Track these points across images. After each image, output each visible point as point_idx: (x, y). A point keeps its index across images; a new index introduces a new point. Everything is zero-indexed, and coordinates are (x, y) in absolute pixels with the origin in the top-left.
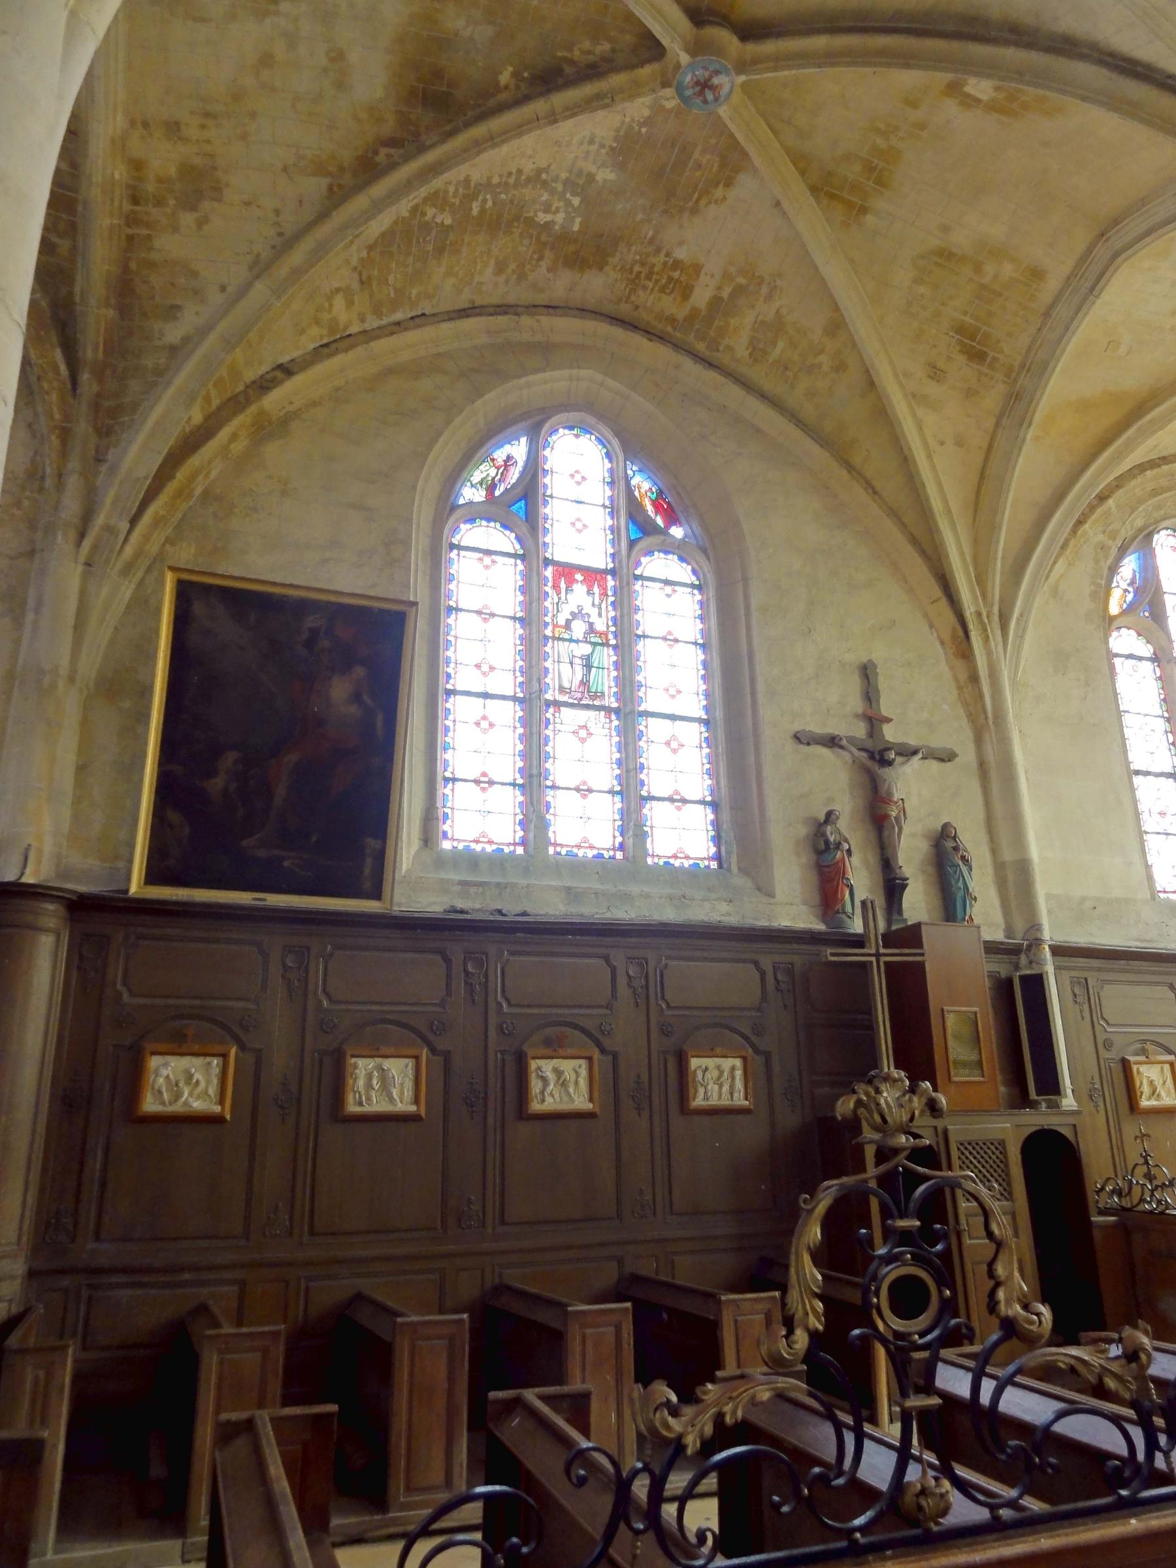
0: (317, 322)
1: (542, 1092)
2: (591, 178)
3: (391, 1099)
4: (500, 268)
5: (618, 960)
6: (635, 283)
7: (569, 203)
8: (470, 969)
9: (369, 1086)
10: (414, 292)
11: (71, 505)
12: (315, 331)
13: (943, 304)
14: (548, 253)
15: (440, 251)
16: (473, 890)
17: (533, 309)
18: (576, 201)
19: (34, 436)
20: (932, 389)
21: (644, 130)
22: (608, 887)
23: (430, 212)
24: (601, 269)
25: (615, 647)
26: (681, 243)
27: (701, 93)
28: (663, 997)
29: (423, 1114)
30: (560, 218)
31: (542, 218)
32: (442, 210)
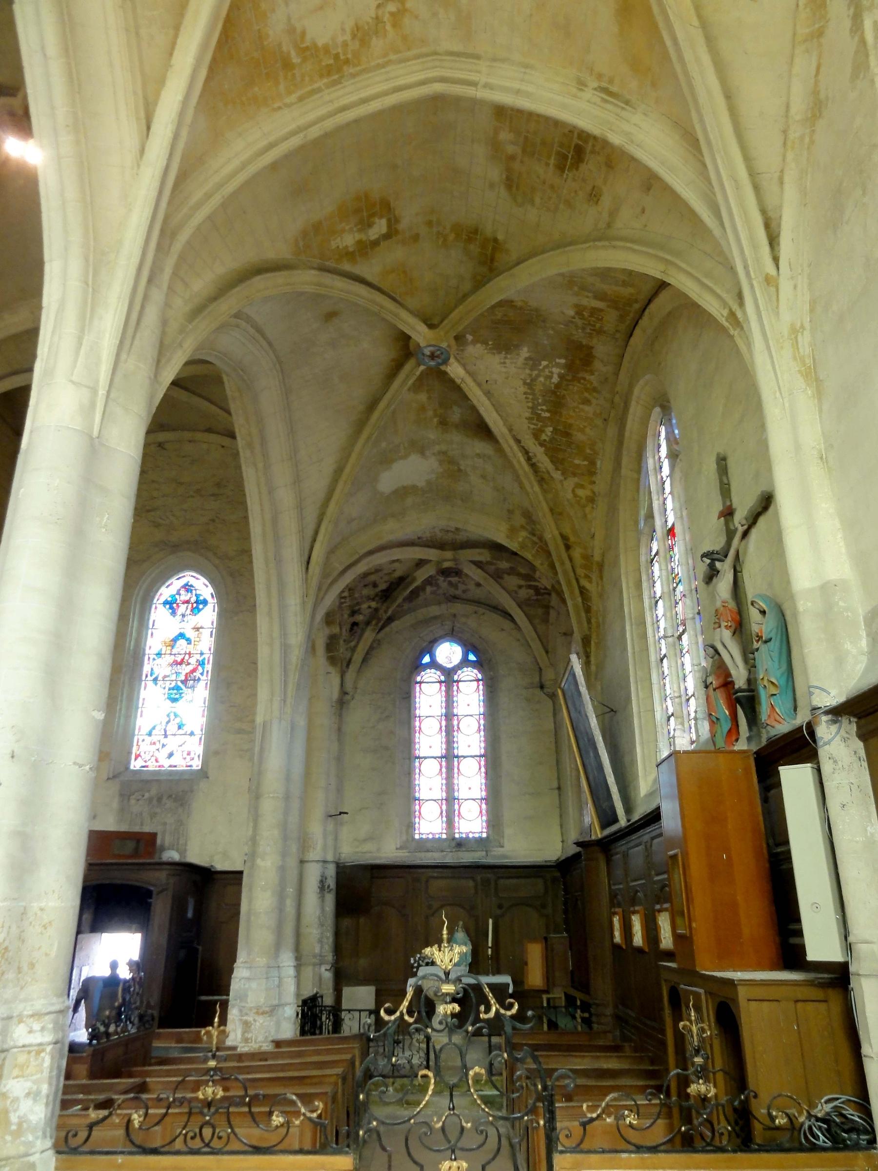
0: (584, 506)
2: (526, 359)
4: (587, 402)
6: (600, 332)
7: (546, 367)
10: (588, 451)
13: (544, 183)
14: (580, 375)
15: (567, 434)
18: (544, 363)
20: (606, 201)
21: (490, 343)
23: (544, 437)
24: (592, 348)
27: (438, 357)
30: (556, 370)
31: (555, 379)
32: (543, 431)
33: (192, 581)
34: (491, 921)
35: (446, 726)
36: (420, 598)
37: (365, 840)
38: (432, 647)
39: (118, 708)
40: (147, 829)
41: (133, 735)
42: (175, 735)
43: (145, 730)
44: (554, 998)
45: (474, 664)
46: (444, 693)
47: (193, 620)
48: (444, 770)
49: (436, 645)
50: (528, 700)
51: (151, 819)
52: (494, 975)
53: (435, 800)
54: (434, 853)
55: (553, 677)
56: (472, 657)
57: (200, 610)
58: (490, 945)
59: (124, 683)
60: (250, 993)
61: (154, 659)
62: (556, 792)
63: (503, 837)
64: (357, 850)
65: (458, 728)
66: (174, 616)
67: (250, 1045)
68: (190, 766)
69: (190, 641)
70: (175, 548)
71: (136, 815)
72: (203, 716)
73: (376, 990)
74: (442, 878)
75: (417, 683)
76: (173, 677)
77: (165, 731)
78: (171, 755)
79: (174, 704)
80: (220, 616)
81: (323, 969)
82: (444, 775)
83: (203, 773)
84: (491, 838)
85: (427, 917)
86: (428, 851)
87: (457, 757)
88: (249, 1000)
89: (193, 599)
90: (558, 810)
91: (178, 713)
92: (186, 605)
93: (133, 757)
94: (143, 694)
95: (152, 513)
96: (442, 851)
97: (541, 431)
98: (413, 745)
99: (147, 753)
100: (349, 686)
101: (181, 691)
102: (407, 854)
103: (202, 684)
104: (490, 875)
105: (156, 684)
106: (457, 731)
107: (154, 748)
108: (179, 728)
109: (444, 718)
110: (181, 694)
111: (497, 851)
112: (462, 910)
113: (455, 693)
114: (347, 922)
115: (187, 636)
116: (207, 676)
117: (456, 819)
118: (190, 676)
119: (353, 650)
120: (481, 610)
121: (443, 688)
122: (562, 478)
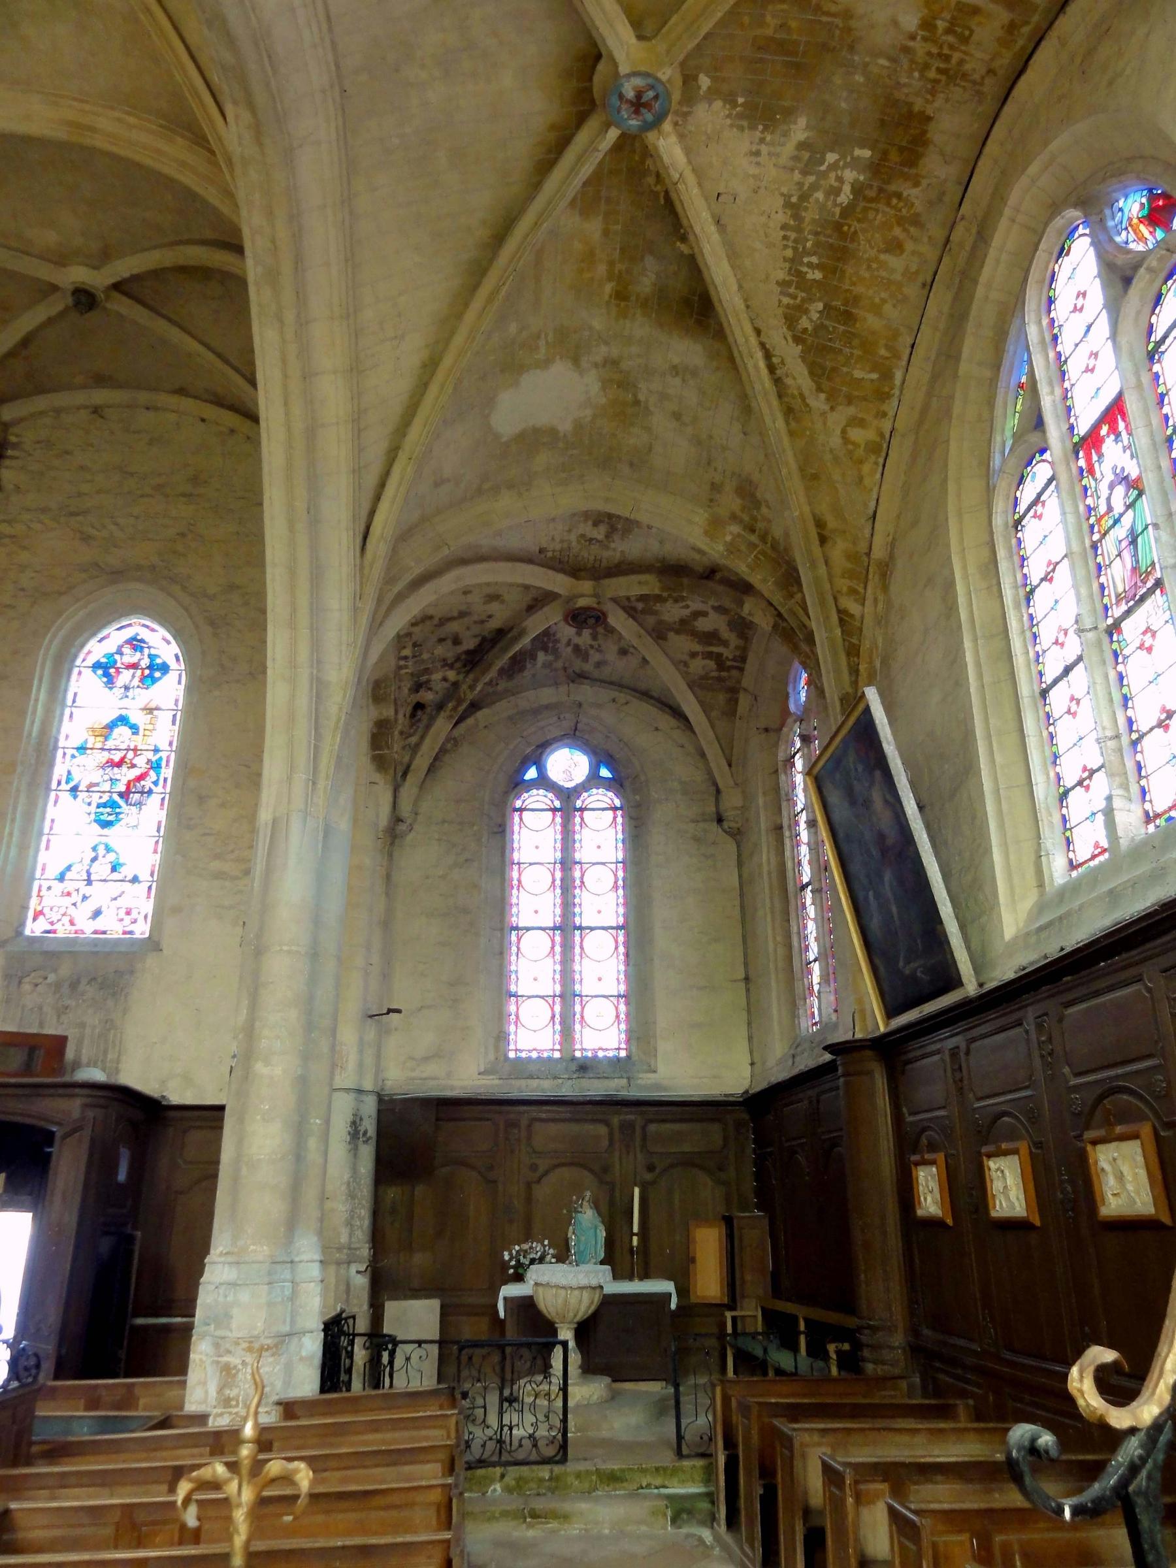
0: (861, 462)
2: (802, 146)
4: (895, 247)
6: (953, 75)
7: (834, 166)
10: (883, 352)
12: (866, 468)
14: (893, 187)
15: (848, 317)
18: (831, 157)
21: (741, 100)
23: (804, 323)
24: (929, 119)
26: (895, 23)
27: (647, 106)
30: (849, 175)
31: (845, 197)
32: (806, 312)
33: (144, 634)
34: (637, 1191)
35: (562, 880)
36: (526, 673)
37: (426, 1059)
38: (541, 754)
39: (7, 830)
40: (50, 1030)
41: (33, 879)
42: (105, 881)
43: (53, 871)
44: (743, 1317)
45: (608, 784)
46: (559, 828)
47: (143, 697)
48: (558, 949)
49: (548, 750)
50: (696, 839)
51: (59, 1017)
52: (641, 1279)
53: (542, 997)
54: (542, 1082)
55: (740, 803)
56: (605, 773)
57: (155, 680)
58: (636, 1229)
59: (18, 790)
60: (235, 1311)
61: (73, 756)
62: (742, 985)
63: (655, 1056)
64: (413, 1074)
65: (582, 882)
66: (111, 688)
67: (234, 1410)
68: (131, 933)
69: (137, 729)
70: (117, 575)
71: (32, 1009)
72: (155, 851)
73: (442, 1307)
74: (554, 1120)
75: (516, 810)
76: (106, 786)
77: (89, 874)
78: (97, 913)
79: (106, 831)
80: (189, 690)
81: (353, 1268)
82: (558, 957)
83: (153, 944)
84: (635, 1058)
85: (529, 1185)
86: (531, 1077)
87: (580, 928)
88: (234, 1325)
89: (145, 662)
90: (744, 1015)
91: (112, 845)
92: (132, 671)
93: (31, 914)
94: (51, 812)
95: (80, 518)
96: (555, 1078)
97: (802, 310)
98: (507, 907)
99: (55, 909)
100: (405, 809)
101: (118, 810)
102: (497, 1082)
103: (154, 801)
104: (630, 1116)
105: (75, 797)
106: (581, 887)
107: (67, 901)
108: (114, 869)
109: (558, 866)
110: (118, 814)
111: (646, 1079)
112: (586, 1173)
113: (577, 828)
114: (392, 1193)
115: (133, 720)
116: (164, 787)
117: (577, 1027)
118: (135, 786)
119: (415, 749)
120: (622, 697)
121: (558, 820)
122: (827, 408)
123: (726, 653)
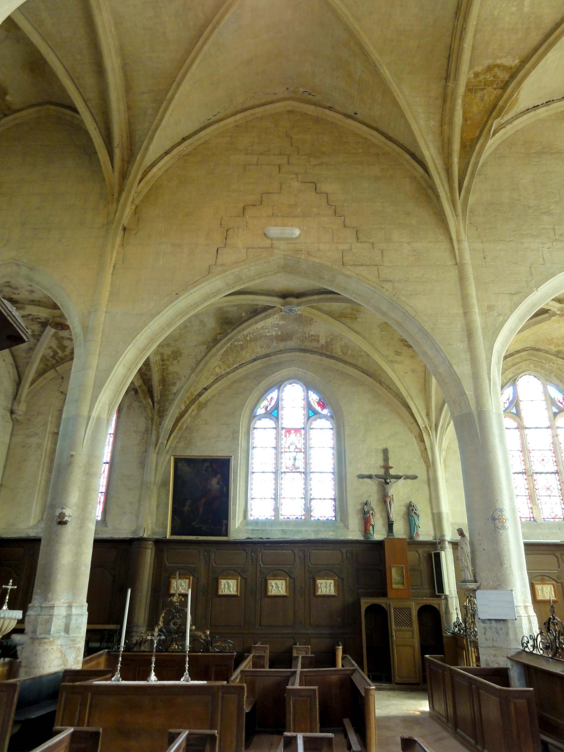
1: (272, 590)
3: (230, 591)
5: (296, 551)
6: (303, 341)
8: (253, 555)
9: (225, 587)
10: (238, 360)
11: (154, 438)
12: (212, 377)
13: (393, 335)
14: (274, 340)
16: (255, 532)
17: (275, 353)
19: (146, 420)
20: (399, 358)
22: (295, 529)
23: (236, 343)
25: (303, 452)
26: (311, 331)
28: (309, 562)
29: (239, 595)
31: (268, 334)
122: (219, 359)
123: (60, 354)
